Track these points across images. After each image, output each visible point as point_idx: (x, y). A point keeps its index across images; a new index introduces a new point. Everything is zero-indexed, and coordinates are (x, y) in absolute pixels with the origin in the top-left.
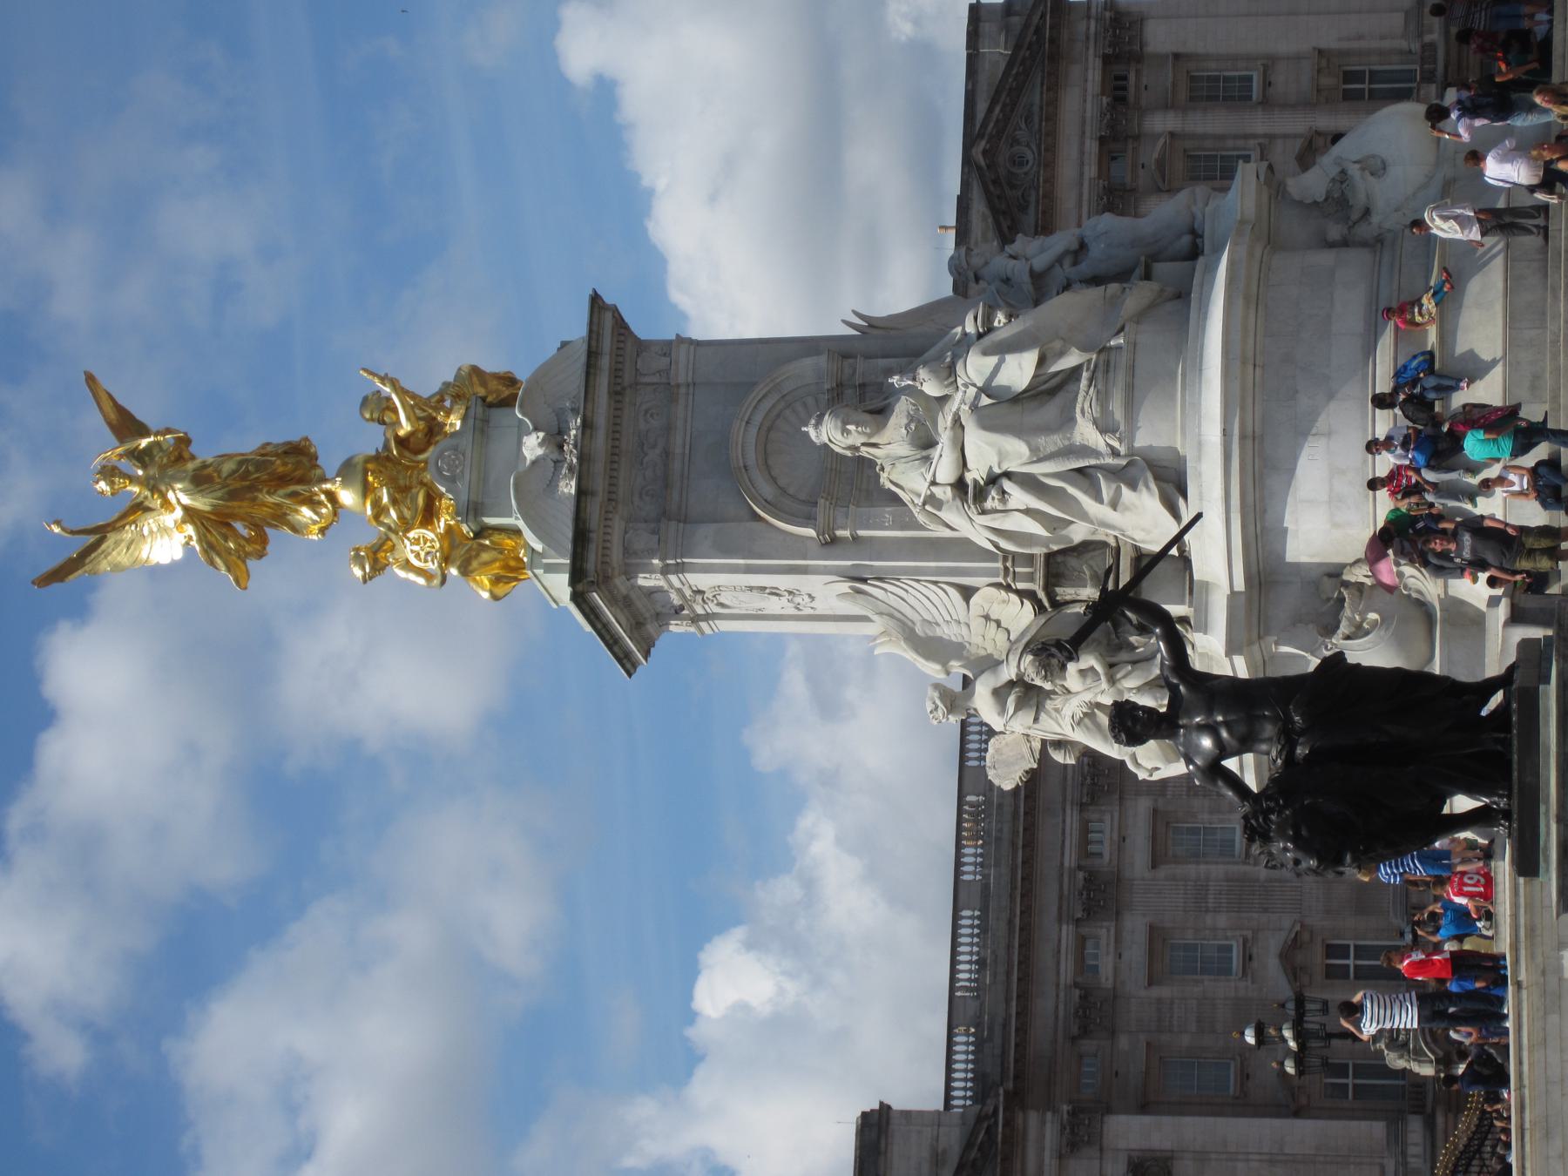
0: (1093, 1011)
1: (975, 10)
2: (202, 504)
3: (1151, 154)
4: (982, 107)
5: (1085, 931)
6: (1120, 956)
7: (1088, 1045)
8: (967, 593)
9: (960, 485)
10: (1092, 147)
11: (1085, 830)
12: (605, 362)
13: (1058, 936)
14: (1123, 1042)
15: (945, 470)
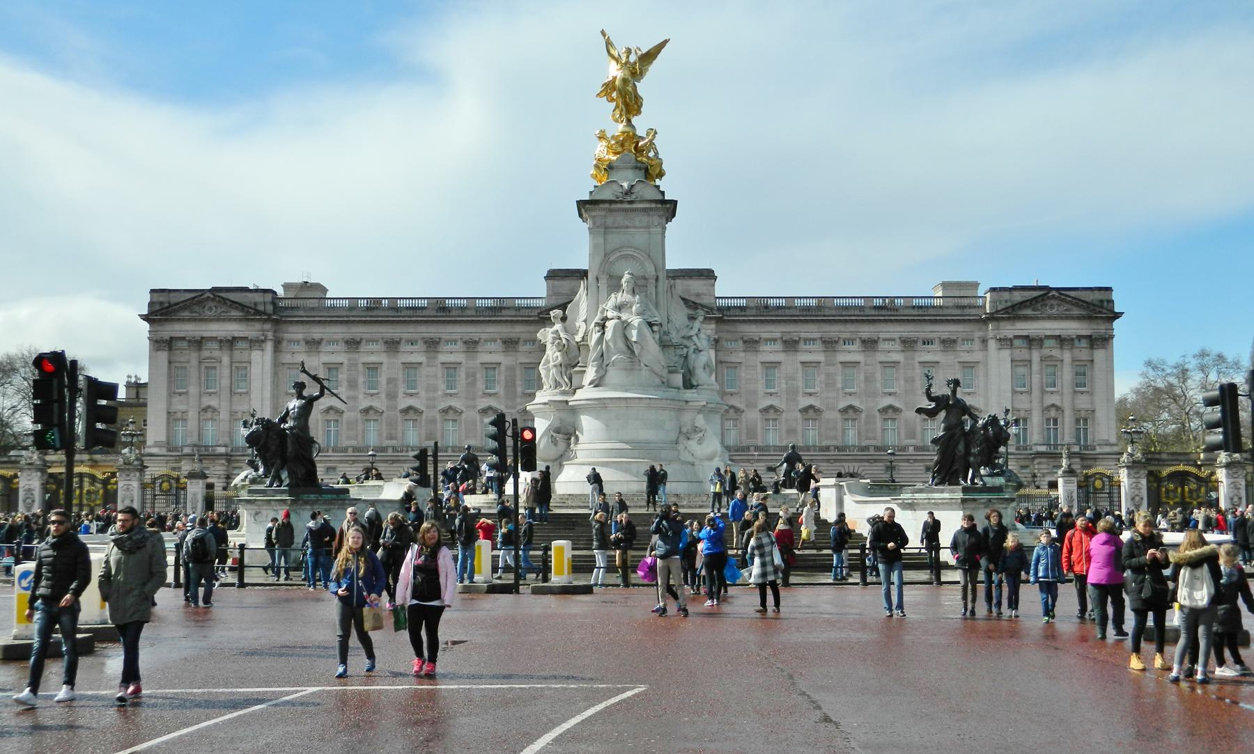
0: (751, 344)
1: (1108, 289)
2: (617, 83)
3: (1056, 353)
4: (1072, 294)
5: (779, 342)
6: (771, 352)
7: (740, 343)
8: (585, 321)
9: (606, 319)
10: (1057, 333)
11: (814, 340)
12: (653, 205)
13: (776, 331)
14: (742, 354)
15: (610, 315)
